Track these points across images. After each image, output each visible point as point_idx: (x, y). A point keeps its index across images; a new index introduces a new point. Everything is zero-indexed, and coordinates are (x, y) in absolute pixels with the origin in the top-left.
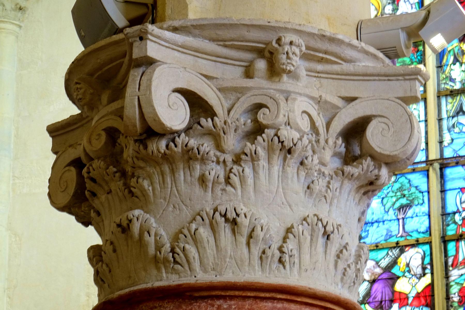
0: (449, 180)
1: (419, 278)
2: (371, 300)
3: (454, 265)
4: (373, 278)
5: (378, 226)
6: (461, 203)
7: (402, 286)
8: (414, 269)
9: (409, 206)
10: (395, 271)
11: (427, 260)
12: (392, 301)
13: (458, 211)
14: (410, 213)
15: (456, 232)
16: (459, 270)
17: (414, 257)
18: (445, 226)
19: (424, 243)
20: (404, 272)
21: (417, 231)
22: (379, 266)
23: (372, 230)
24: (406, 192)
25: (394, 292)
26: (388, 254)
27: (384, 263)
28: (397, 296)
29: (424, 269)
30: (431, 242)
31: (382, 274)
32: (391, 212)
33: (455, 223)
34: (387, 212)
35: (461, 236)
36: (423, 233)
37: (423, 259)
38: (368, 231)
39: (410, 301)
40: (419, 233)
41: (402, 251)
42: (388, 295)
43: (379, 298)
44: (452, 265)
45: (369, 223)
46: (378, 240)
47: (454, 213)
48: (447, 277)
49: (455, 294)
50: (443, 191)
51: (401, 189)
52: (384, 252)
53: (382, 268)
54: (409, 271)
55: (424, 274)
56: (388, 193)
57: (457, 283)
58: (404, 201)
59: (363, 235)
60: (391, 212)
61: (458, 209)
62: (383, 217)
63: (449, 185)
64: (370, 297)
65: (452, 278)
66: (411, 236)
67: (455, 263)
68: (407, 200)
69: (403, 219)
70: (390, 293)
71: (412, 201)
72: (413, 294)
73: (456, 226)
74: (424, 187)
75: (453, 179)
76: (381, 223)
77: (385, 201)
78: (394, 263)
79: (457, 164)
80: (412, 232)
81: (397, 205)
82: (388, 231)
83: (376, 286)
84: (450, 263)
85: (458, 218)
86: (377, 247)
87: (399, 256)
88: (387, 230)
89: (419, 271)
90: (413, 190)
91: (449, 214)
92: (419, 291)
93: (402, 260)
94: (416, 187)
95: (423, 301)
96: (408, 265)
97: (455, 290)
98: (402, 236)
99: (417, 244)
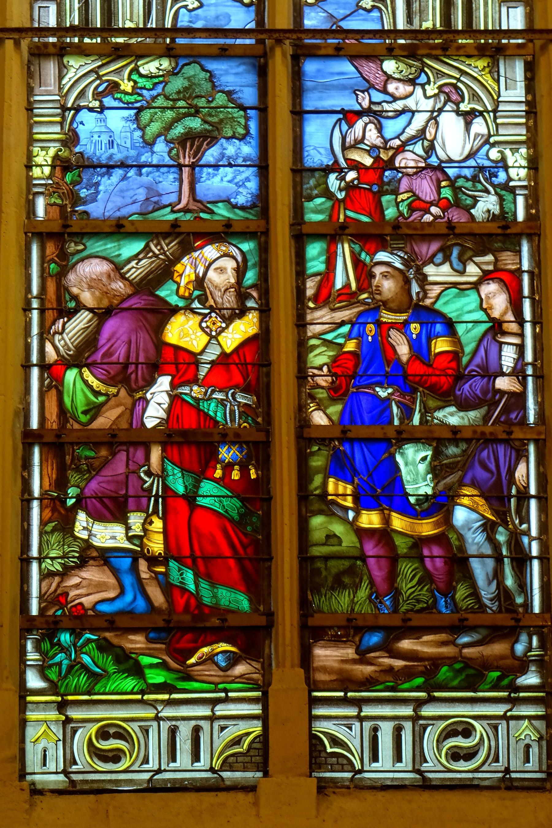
0: (314, 89)
1: (229, 320)
2: (98, 356)
3: (325, 296)
4: (105, 303)
5: (124, 178)
6: (344, 148)
7: (184, 332)
8: (218, 294)
9: (209, 137)
10: (167, 292)
11: (250, 277)
12: (154, 370)
13: (335, 168)
14: (211, 155)
15: (330, 216)
16: (333, 310)
17: (216, 265)
18: (299, 200)
19: (246, 235)
20: (189, 299)
21: (227, 201)
22: (123, 277)
23: (108, 183)
24: (202, 103)
25: (161, 345)
26: (147, 249)
27: (135, 271)
28: (169, 355)
29: (242, 296)
30: (266, 233)
31: (130, 296)
32: (161, 147)
33: (328, 194)
34: (150, 144)
35: (343, 227)
36: (243, 208)
37: (240, 271)
38: (98, 184)
39: (204, 370)
40: (235, 206)
41: (186, 248)
42: (146, 350)
43: (120, 354)
44: (316, 298)
45: (101, 166)
46: (124, 212)
47: (327, 170)
48: (301, 324)
49: (320, 368)
50: (299, 114)
51: (187, 93)
52: (137, 246)
53: (131, 282)
54: (203, 299)
55: (241, 312)
56: (154, 98)
57: (328, 343)
58: (195, 123)
59: (83, 193)
60: (161, 147)
61: (336, 162)
62: (139, 155)
63: (310, 103)
64: (97, 350)
65: (313, 329)
66: (212, 212)
67: (325, 292)
68: (205, 122)
69: (193, 166)
70: (150, 346)
71: (217, 127)
72: (212, 354)
73: (329, 204)
74: (249, 96)
75: (327, 88)
76: (132, 173)
77: (146, 116)
78: (165, 273)
79: (338, 53)
80: (214, 202)
81: (178, 130)
82: (152, 191)
83: (111, 325)
84: (310, 292)
85: (333, 182)
86: (119, 229)
87: (177, 259)
88: (149, 188)
89: (229, 300)
90: (220, 99)
91: (313, 170)
92: (228, 350)
93: (186, 270)
94: (229, 94)
95: (238, 378)
96: (200, 282)
97: (319, 358)
98: (186, 210)
99: (223, 233)
